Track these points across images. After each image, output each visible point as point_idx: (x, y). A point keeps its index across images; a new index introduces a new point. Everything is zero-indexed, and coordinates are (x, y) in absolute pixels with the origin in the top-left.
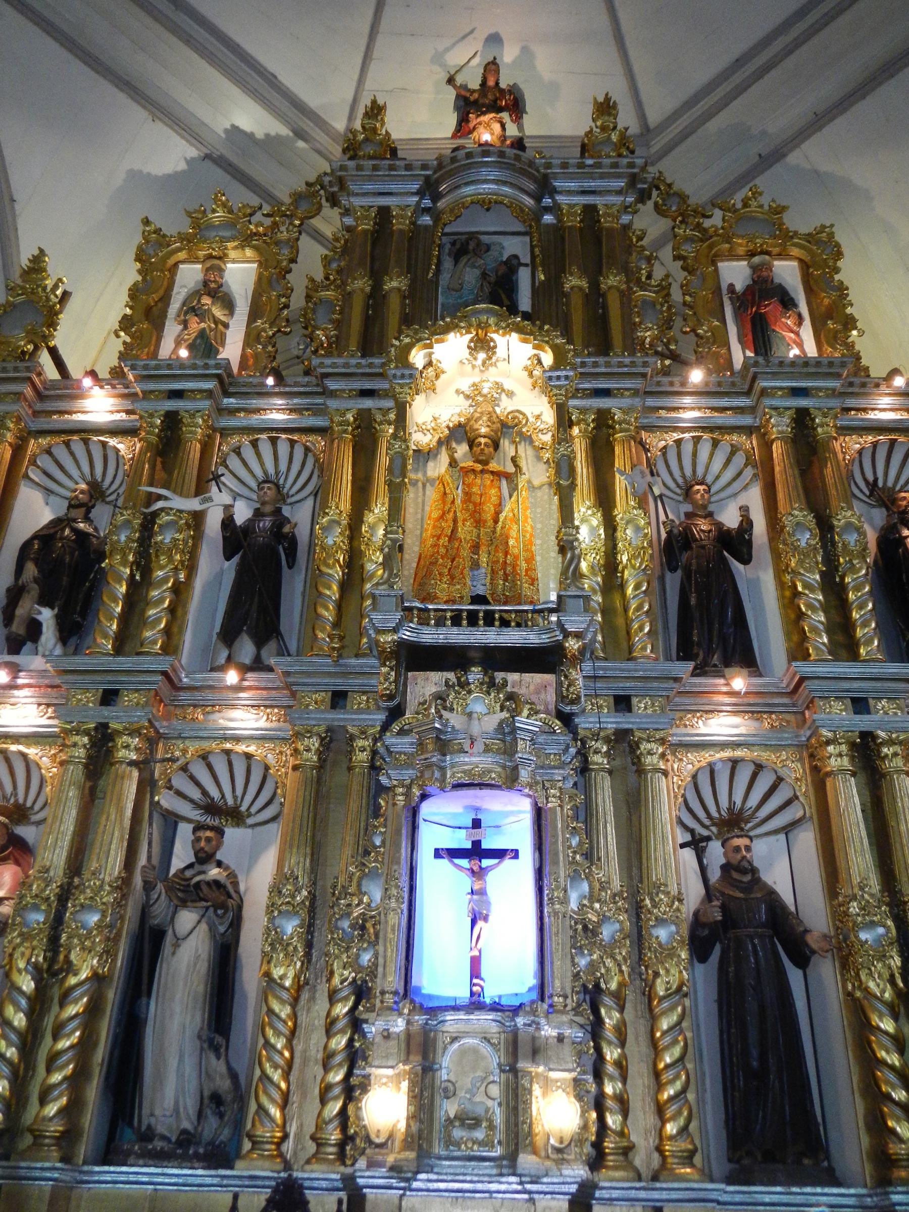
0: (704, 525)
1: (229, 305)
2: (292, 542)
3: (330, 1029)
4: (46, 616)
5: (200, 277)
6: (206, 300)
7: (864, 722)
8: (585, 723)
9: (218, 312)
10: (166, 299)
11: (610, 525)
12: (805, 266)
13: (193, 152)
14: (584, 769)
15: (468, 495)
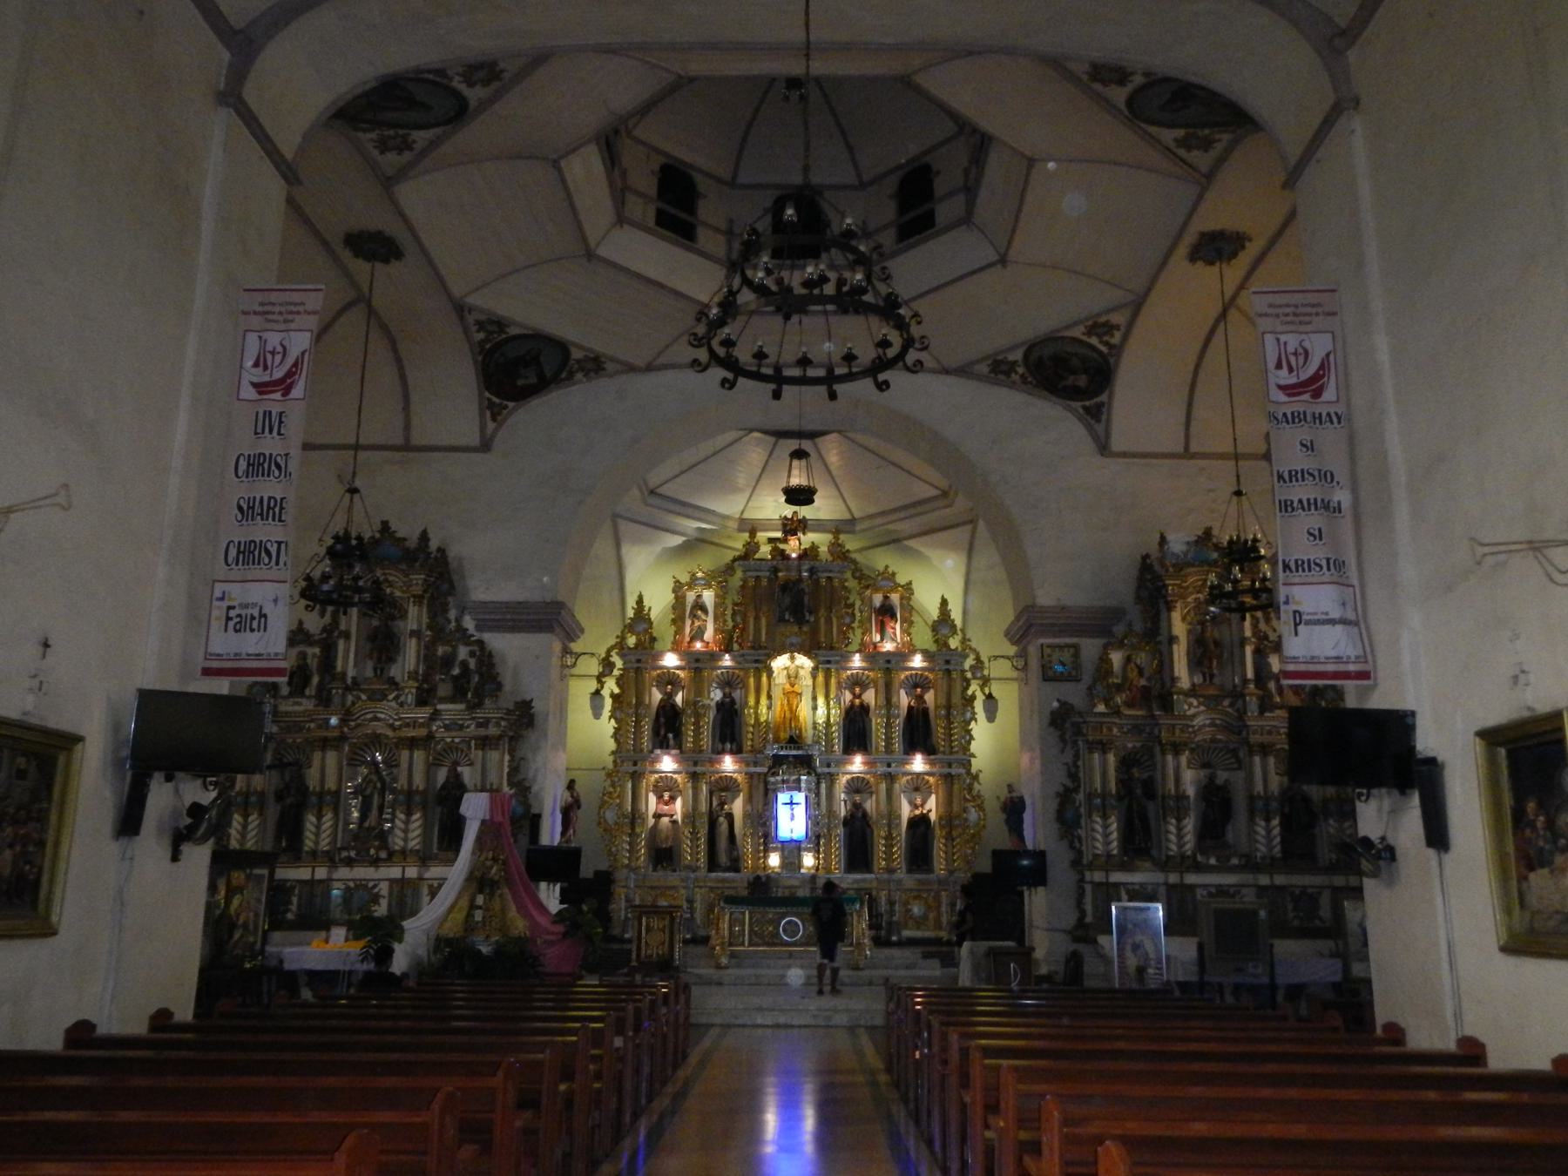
0: (857, 701)
1: (705, 611)
2: (736, 711)
3: (759, 845)
4: (671, 735)
5: (694, 598)
6: (699, 612)
7: (890, 770)
8: (819, 770)
9: (704, 617)
10: (685, 611)
11: (829, 709)
12: (902, 598)
13: (684, 539)
14: (818, 784)
15: (788, 701)
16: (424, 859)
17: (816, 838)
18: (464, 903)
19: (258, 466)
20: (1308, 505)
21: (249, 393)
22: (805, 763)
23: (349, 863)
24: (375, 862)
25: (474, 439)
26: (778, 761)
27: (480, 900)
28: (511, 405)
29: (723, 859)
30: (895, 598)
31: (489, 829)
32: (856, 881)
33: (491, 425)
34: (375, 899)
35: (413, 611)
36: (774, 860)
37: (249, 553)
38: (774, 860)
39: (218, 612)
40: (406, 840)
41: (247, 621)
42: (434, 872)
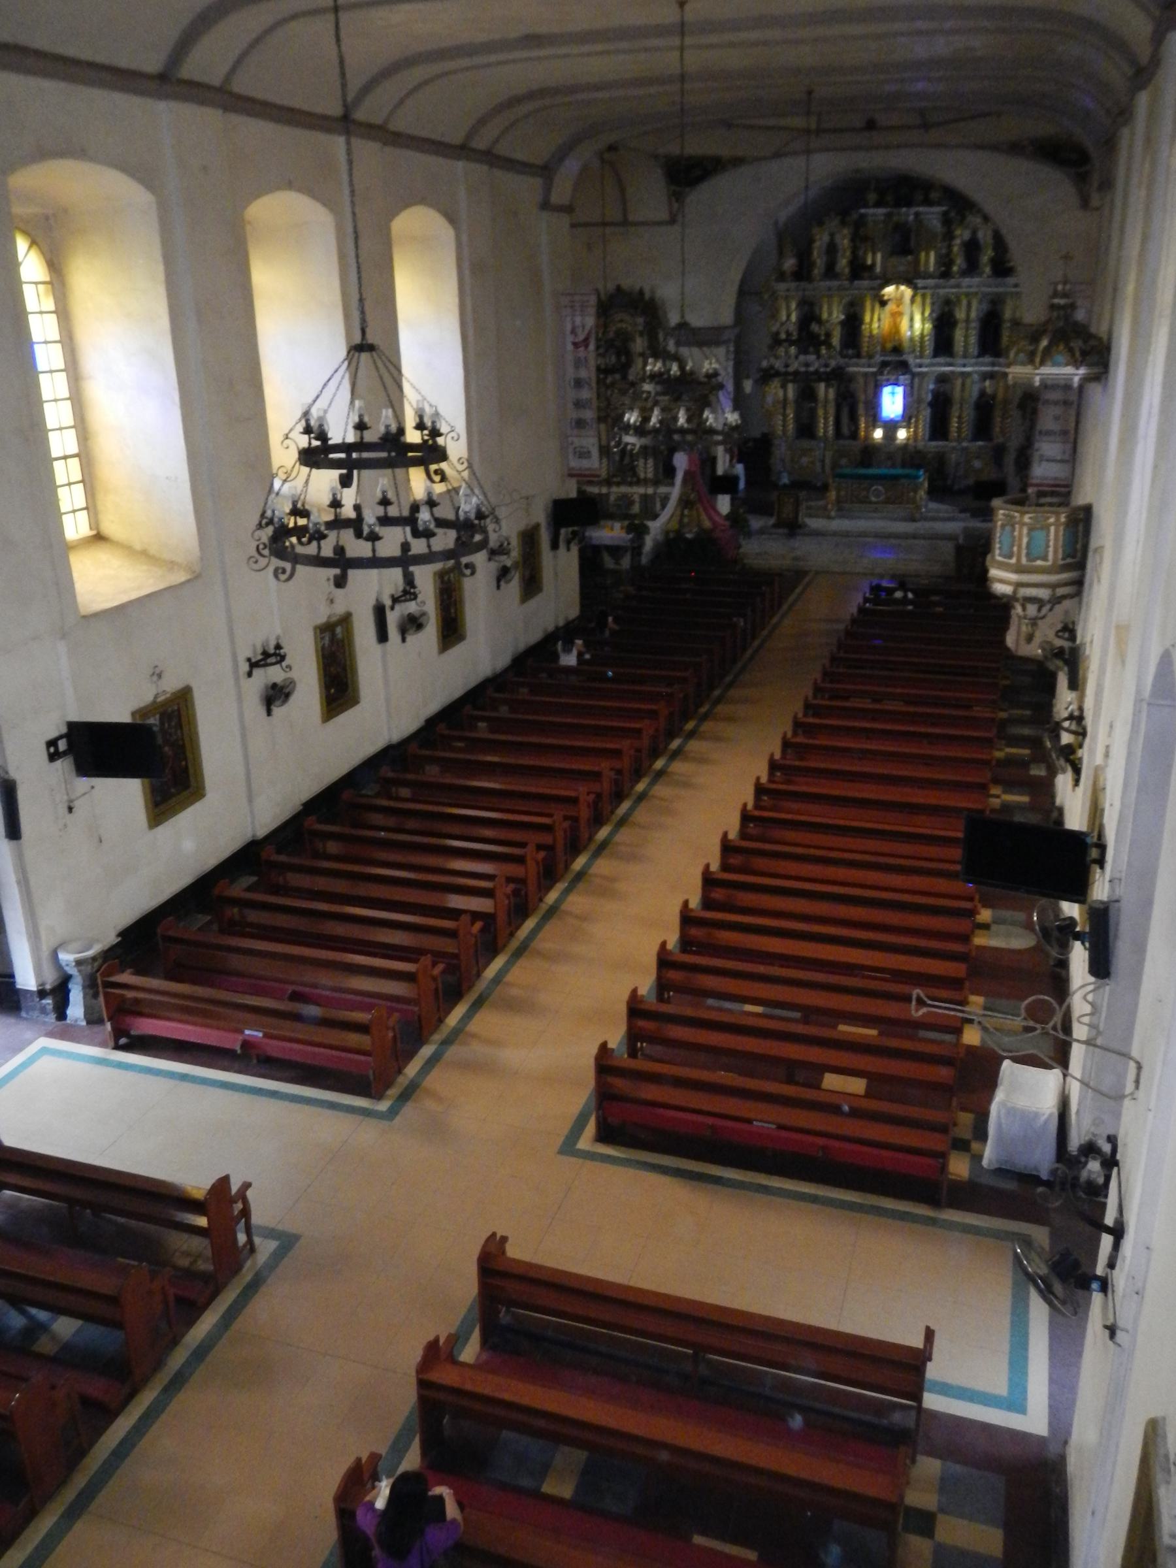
16: (656, 483)
17: (908, 418)
18: (678, 513)
19: (578, 383)
20: (1056, 403)
21: (570, 347)
22: (903, 367)
23: (618, 484)
24: (631, 484)
25: (664, 215)
26: (884, 364)
27: (686, 512)
28: (687, 189)
29: (845, 430)
30: (980, 235)
31: (688, 475)
32: (937, 447)
33: (676, 205)
34: (632, 503)
35: (639, 341)
36: (878, 434)
37: (580, 424)
38: (878, 434)
39: (571, 450)
40: (646, 473)
41: (584, 454)
42: (662, 490)
